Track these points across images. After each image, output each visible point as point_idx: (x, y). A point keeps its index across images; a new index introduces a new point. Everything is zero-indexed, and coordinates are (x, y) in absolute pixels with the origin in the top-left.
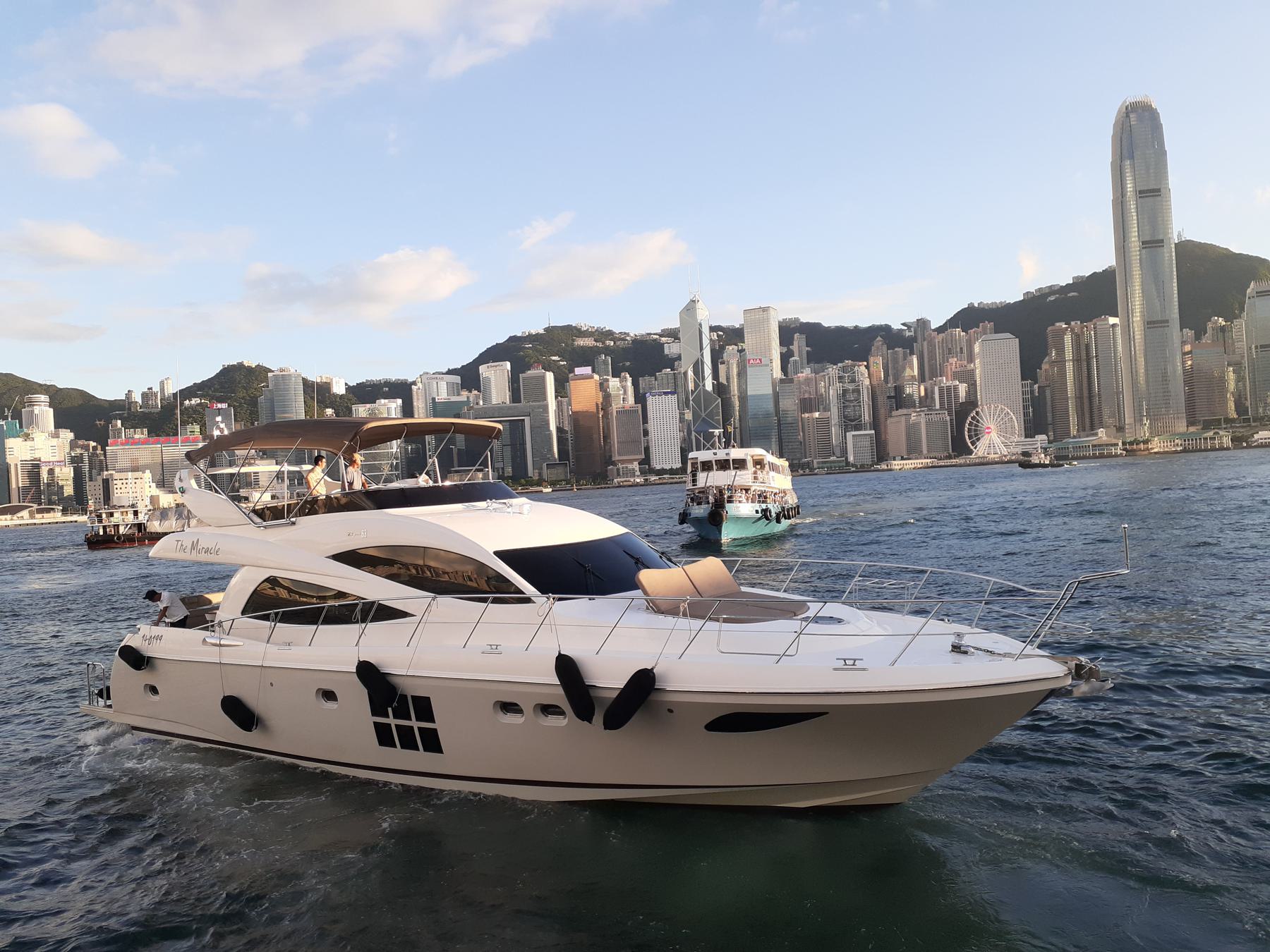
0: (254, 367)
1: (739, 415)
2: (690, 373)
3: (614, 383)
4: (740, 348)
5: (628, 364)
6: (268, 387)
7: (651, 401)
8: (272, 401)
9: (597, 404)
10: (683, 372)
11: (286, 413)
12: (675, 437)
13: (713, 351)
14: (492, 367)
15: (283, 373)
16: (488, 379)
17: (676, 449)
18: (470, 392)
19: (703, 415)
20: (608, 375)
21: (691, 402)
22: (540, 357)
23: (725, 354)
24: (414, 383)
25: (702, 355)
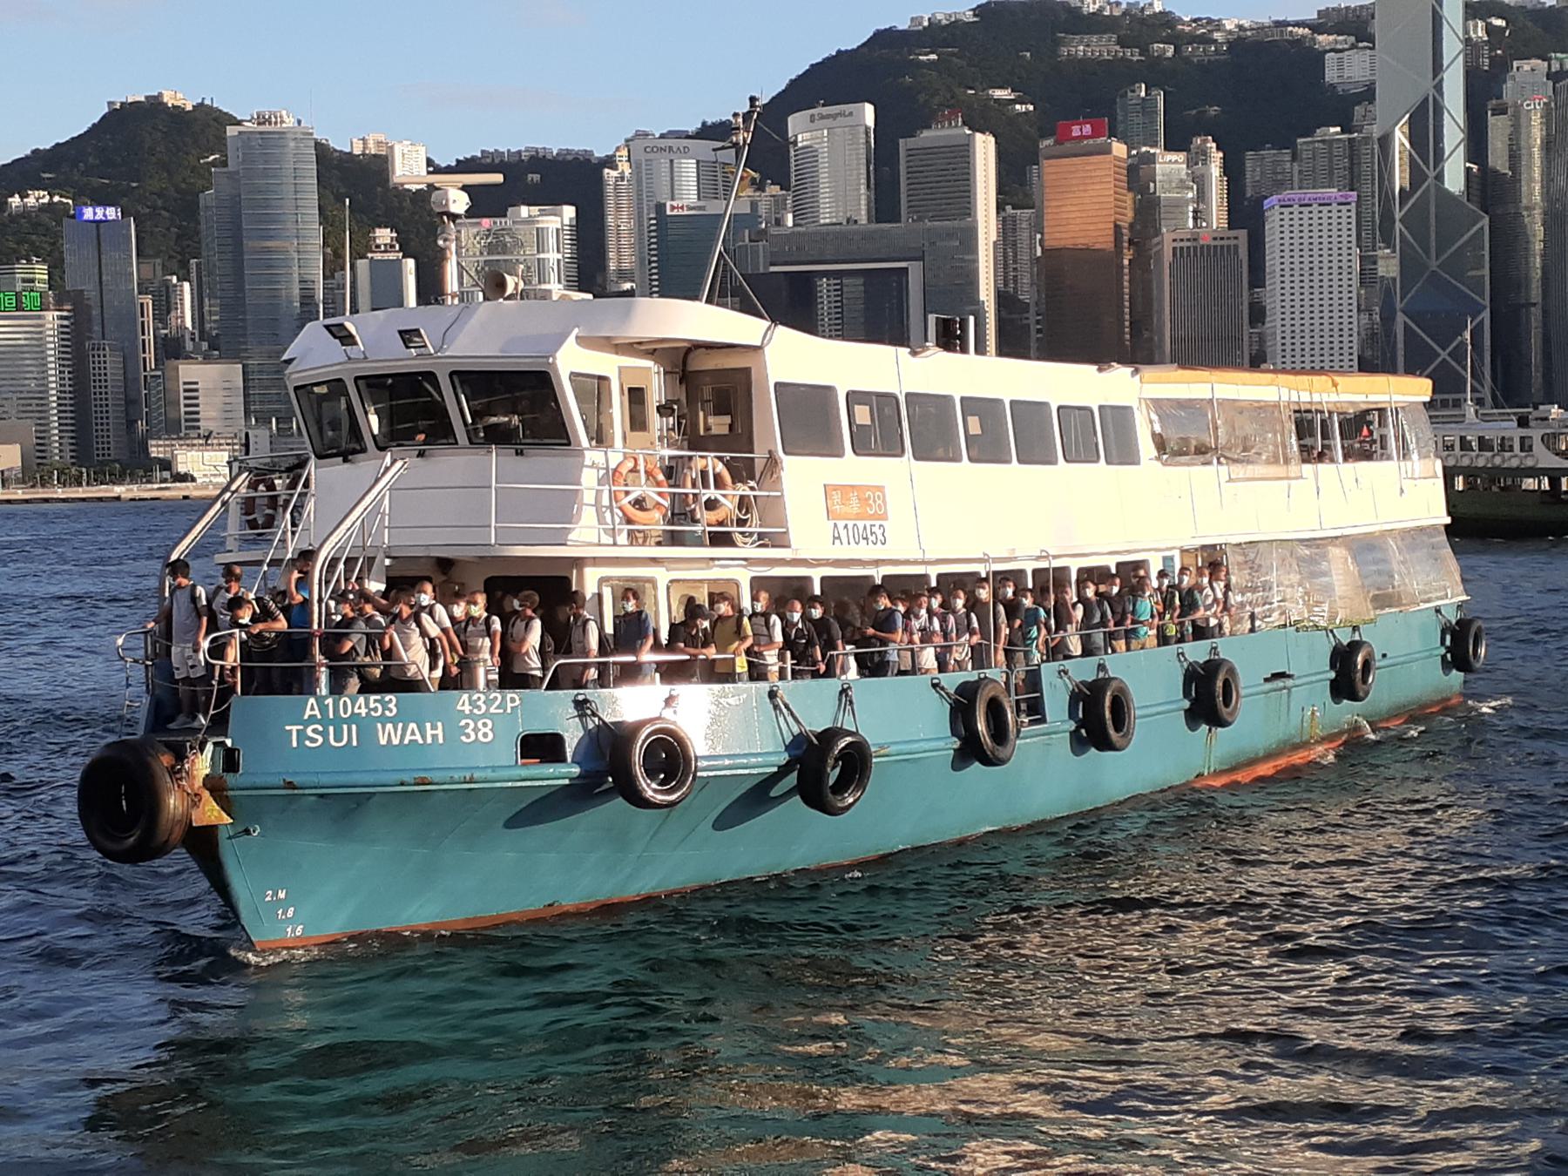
0: (189, 108)
1: (1543, 268)
2: (1400, 138)
3: (1170, 165)
4: (1555, 67)
5: (1214, 110)
6: (225, 164)
7: (1276, 222)
8: (234, 207)
9: (1117, 228)
10: (1376, 136)
11: (271, 238)
12: (1346, 327)
13: (1471, 74)
14: (822, 117)
15: (266, 128)
16: (810, 153)
20: (1155, 145)
21: (1398, 225)
22: (959, 91)
23: (1509, 84)
24: (610, 162)
25: (1439, 88)
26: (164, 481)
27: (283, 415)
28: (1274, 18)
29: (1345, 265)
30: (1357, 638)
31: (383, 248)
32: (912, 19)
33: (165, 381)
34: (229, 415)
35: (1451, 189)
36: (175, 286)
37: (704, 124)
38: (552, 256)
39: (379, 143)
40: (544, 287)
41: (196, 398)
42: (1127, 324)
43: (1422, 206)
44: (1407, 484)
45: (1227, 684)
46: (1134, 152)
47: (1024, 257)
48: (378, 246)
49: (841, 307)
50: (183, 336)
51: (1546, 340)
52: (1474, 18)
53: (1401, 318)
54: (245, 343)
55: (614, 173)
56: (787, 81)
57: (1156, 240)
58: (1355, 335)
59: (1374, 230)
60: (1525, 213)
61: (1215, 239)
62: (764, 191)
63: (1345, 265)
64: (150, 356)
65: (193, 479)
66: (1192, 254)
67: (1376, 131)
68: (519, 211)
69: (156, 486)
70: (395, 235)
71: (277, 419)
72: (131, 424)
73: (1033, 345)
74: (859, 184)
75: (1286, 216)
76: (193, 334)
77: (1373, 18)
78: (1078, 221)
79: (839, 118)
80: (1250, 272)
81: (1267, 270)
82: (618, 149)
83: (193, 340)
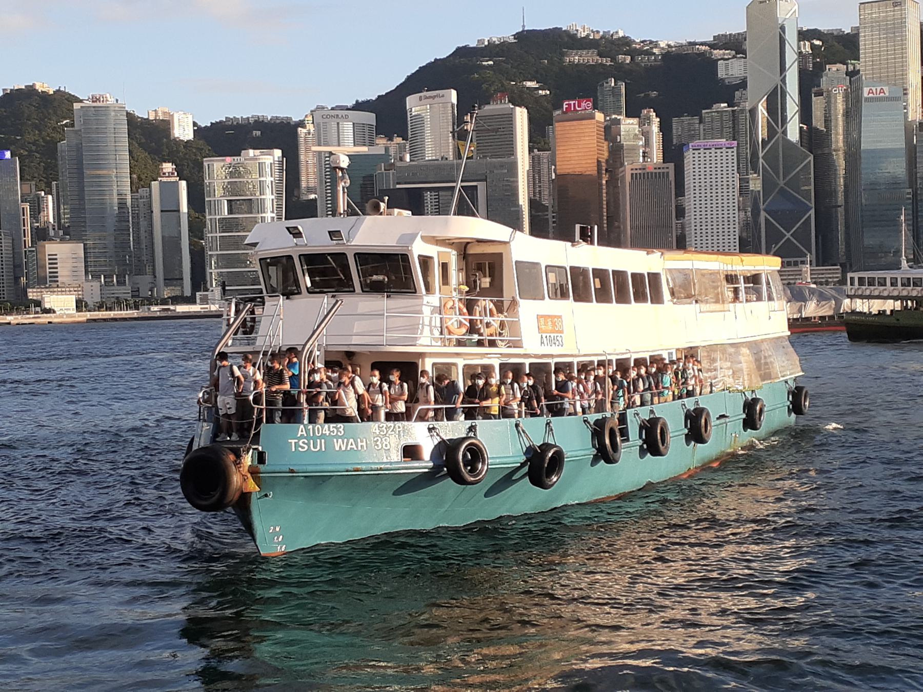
0: (51, 92)
3: (629, 126)
4: (851, 68)
5: (654, 94)
6: (73, 125)
7: (690, 157)
8: (79, 149)
9: (599, 162)
12: (731, 219)
13: (802, 73)
16: (419, 118)
17: (732, 241)
18: (391, 139)
19: (781, 183)
20: (620, 114)
21: (761, 160)
23: (824, 78)
24: (301, 124)
25: (783, 81)
26: (37, 313)
27: (108, 273)
28: (688, 41)
29: (730, 183)
30: (754, 396)
31: (167, 175)
32: (478, 41)
33: (37, 252)
34: (75, 274)
35: (792, 140)
36: (43, 197)
37: (357, 101)
38: (268, 179)
39: (164, 113)
40: (263, 197)
41: (56, 264)
42: (605, 218)
43: (775, 148)
44: (772, 314)
45: (662, 429)
46: (608, 118)
47: (545, 179)
48: (164, 174)
49: (439, 208)
50: (48, 227)
51: (847, 227)
52: (803, 40)
53: (763, 214)
54: (86, 231)
55: (304, 131)
56: (406, 77)
57: (621, 169)
58: (737, 224)
59: (747, 163)
60: (834, 153)
61: (655, 168)
62: (392, 141)
63: (730, 183)
64: (28, 239)
65: (54, 312)
66: (642, 177)
67: (748, 106)
68: (248, 154)
69: (32, 316)
70: (174, 167)
71: (104, 276)
72: (17, 279)
73: (551, 230)
74: (449, 137)
75: (696, 155)
76: (54, 226)
77: (745, 40)
78: (577, 158)
79: (436, 99)
80: (676, 188)
81: (686, 187)
82: (306, 116)
83: (54, 229)
